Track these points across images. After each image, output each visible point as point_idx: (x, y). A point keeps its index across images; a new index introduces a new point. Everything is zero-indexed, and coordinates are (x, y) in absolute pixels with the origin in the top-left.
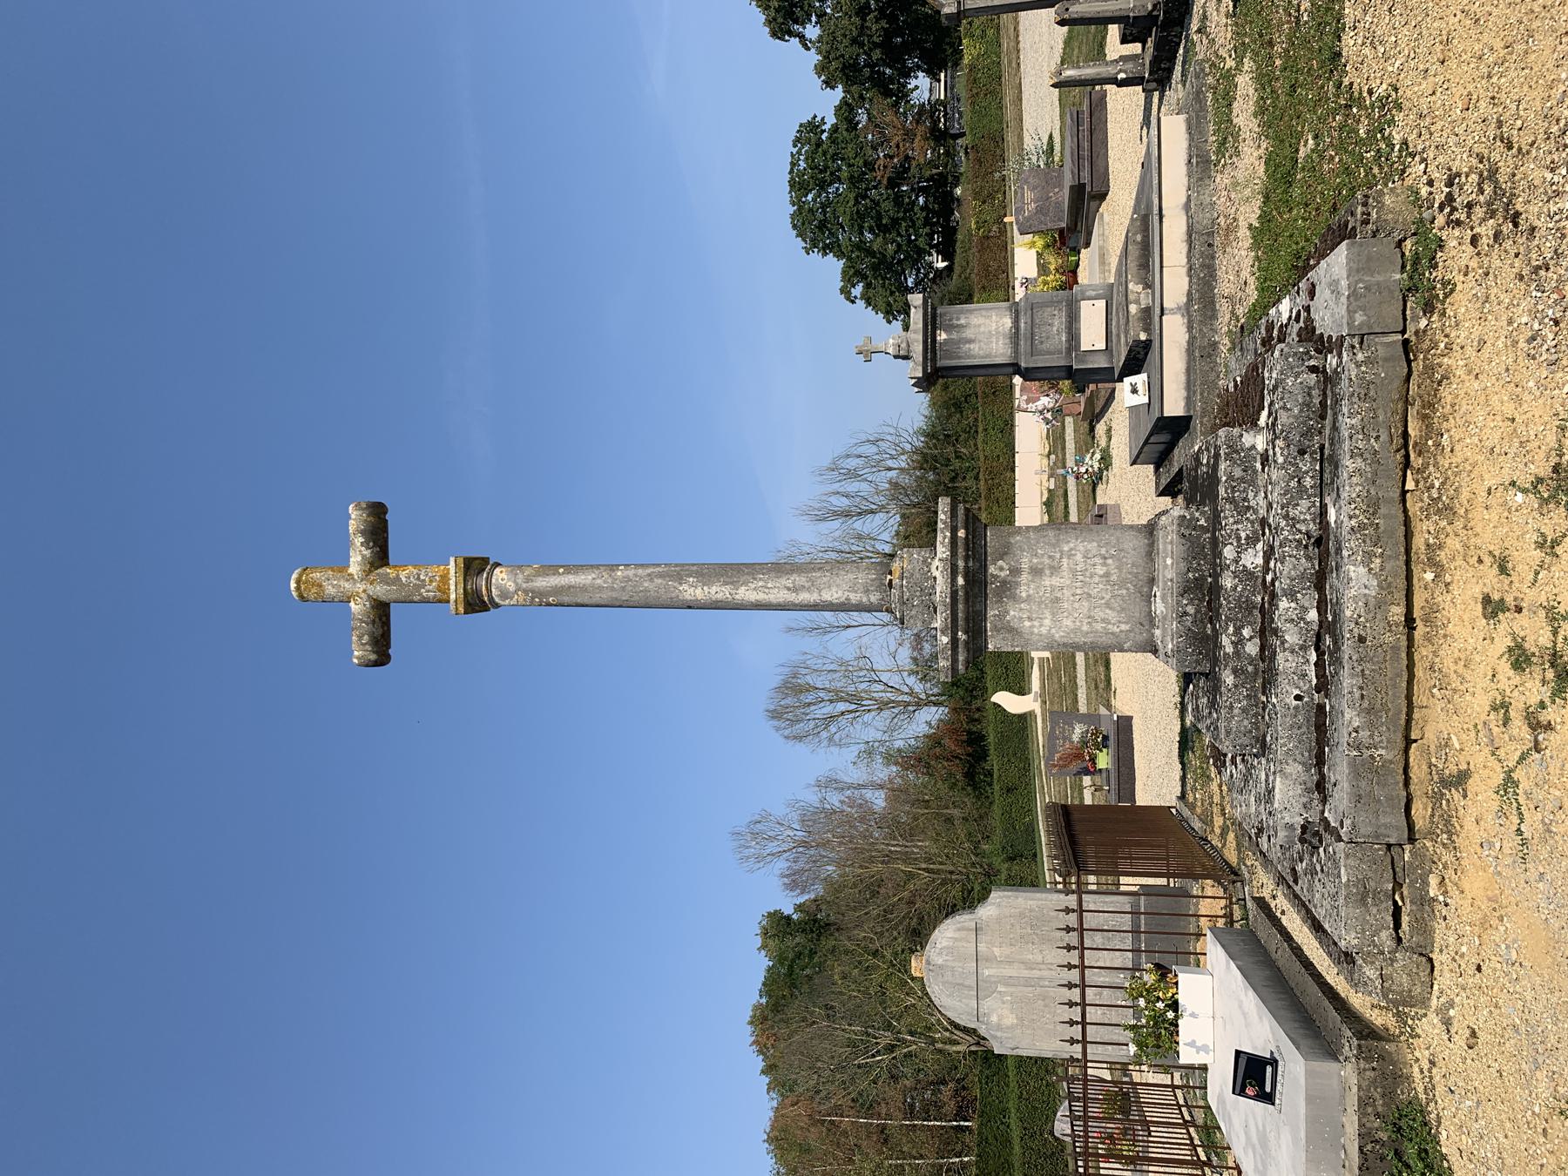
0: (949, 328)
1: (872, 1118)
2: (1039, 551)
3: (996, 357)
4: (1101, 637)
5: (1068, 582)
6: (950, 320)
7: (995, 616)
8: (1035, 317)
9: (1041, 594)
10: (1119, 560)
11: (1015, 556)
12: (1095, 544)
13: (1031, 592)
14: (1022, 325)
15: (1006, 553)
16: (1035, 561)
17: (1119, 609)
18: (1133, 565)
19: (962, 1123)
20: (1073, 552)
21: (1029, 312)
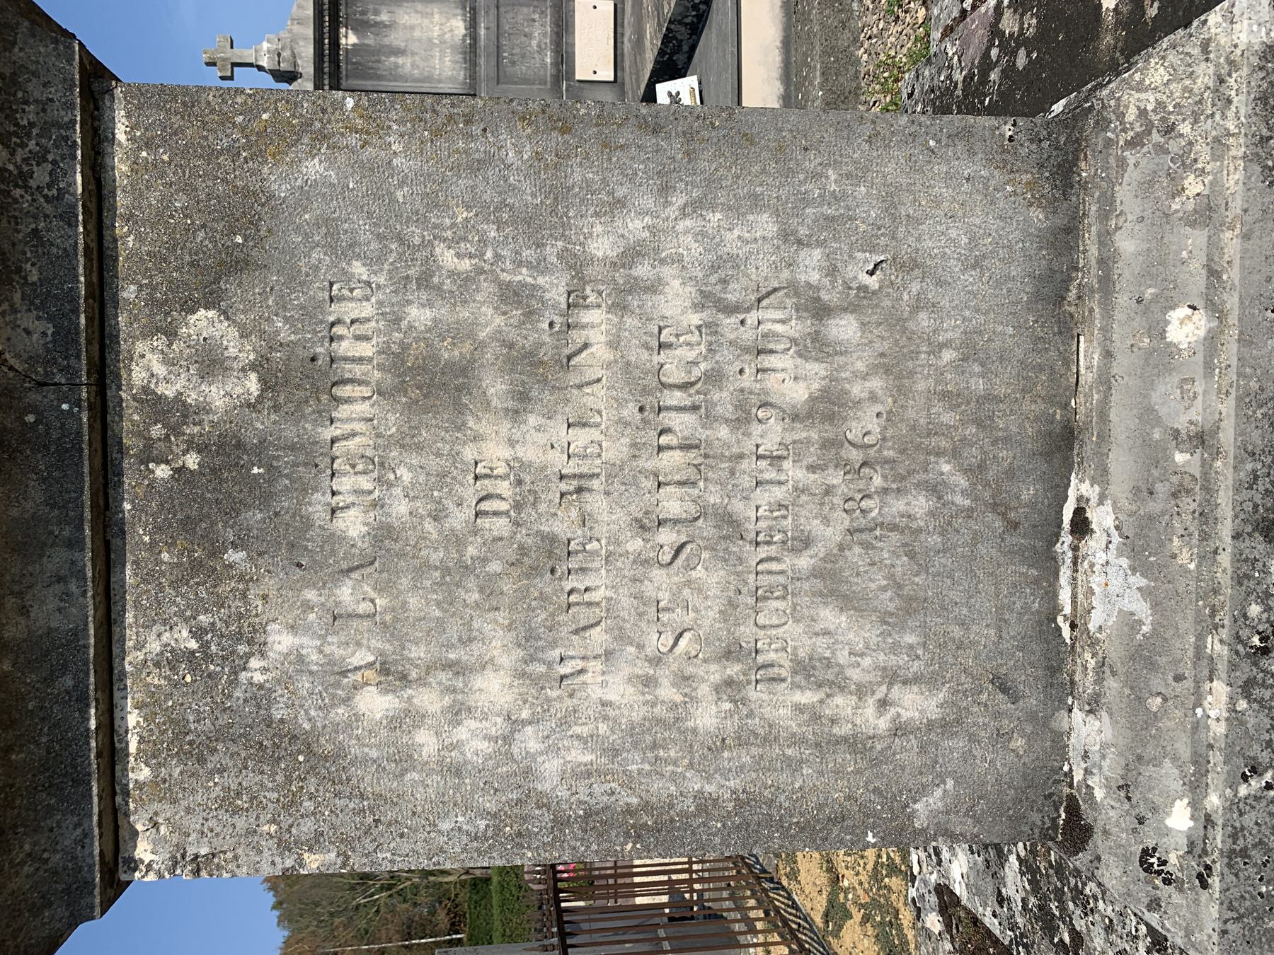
0: (361, 26)
1: (373, 944)
2: (447, 258)
3: (440, 81)
4: (794, 766)
5: (616, 450)
6: (363, 13)
7: (172, 659)
8: (503, 21)
9: (459, 518)
10: (897, 323)
11: (294, 280)
12: (765, 225)
13: (400, 508)
14: (482, 32)
15: (237, 264)
16: (419, 315)
17: (887, 601)
18: (970, 352)
19: (454, 936)
20: (643, 270)
21: (493, 11)
